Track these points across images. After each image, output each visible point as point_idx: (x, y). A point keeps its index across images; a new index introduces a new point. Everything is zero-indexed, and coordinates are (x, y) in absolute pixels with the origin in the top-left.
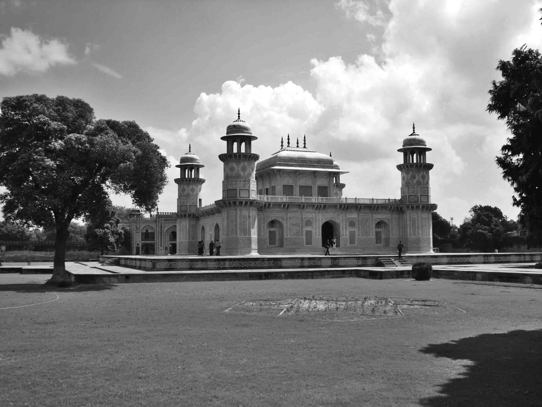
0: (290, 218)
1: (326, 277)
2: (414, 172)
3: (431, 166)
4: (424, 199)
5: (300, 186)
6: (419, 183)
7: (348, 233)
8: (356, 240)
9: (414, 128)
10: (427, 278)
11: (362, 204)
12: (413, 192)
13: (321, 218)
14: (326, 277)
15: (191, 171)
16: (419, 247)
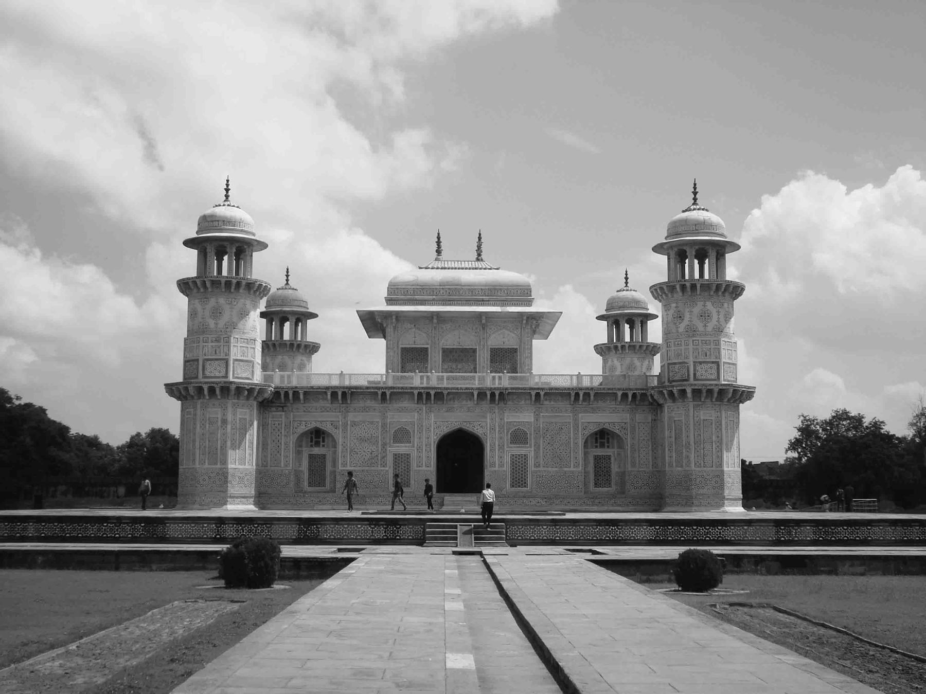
0: (354, 424)
1: (154, 567)
2: (680, 304)
3: (736, 290)
4: (702, 371)
5: (445, 351)
6: (692, 331)
7: (507, 459)
9: (695, 193)
10: (267, 583)
11: (542, 389)
12: (679, 355)
13: (436, 424)
14: (154, 567)
15: (296, 325)
16: (691, 497)
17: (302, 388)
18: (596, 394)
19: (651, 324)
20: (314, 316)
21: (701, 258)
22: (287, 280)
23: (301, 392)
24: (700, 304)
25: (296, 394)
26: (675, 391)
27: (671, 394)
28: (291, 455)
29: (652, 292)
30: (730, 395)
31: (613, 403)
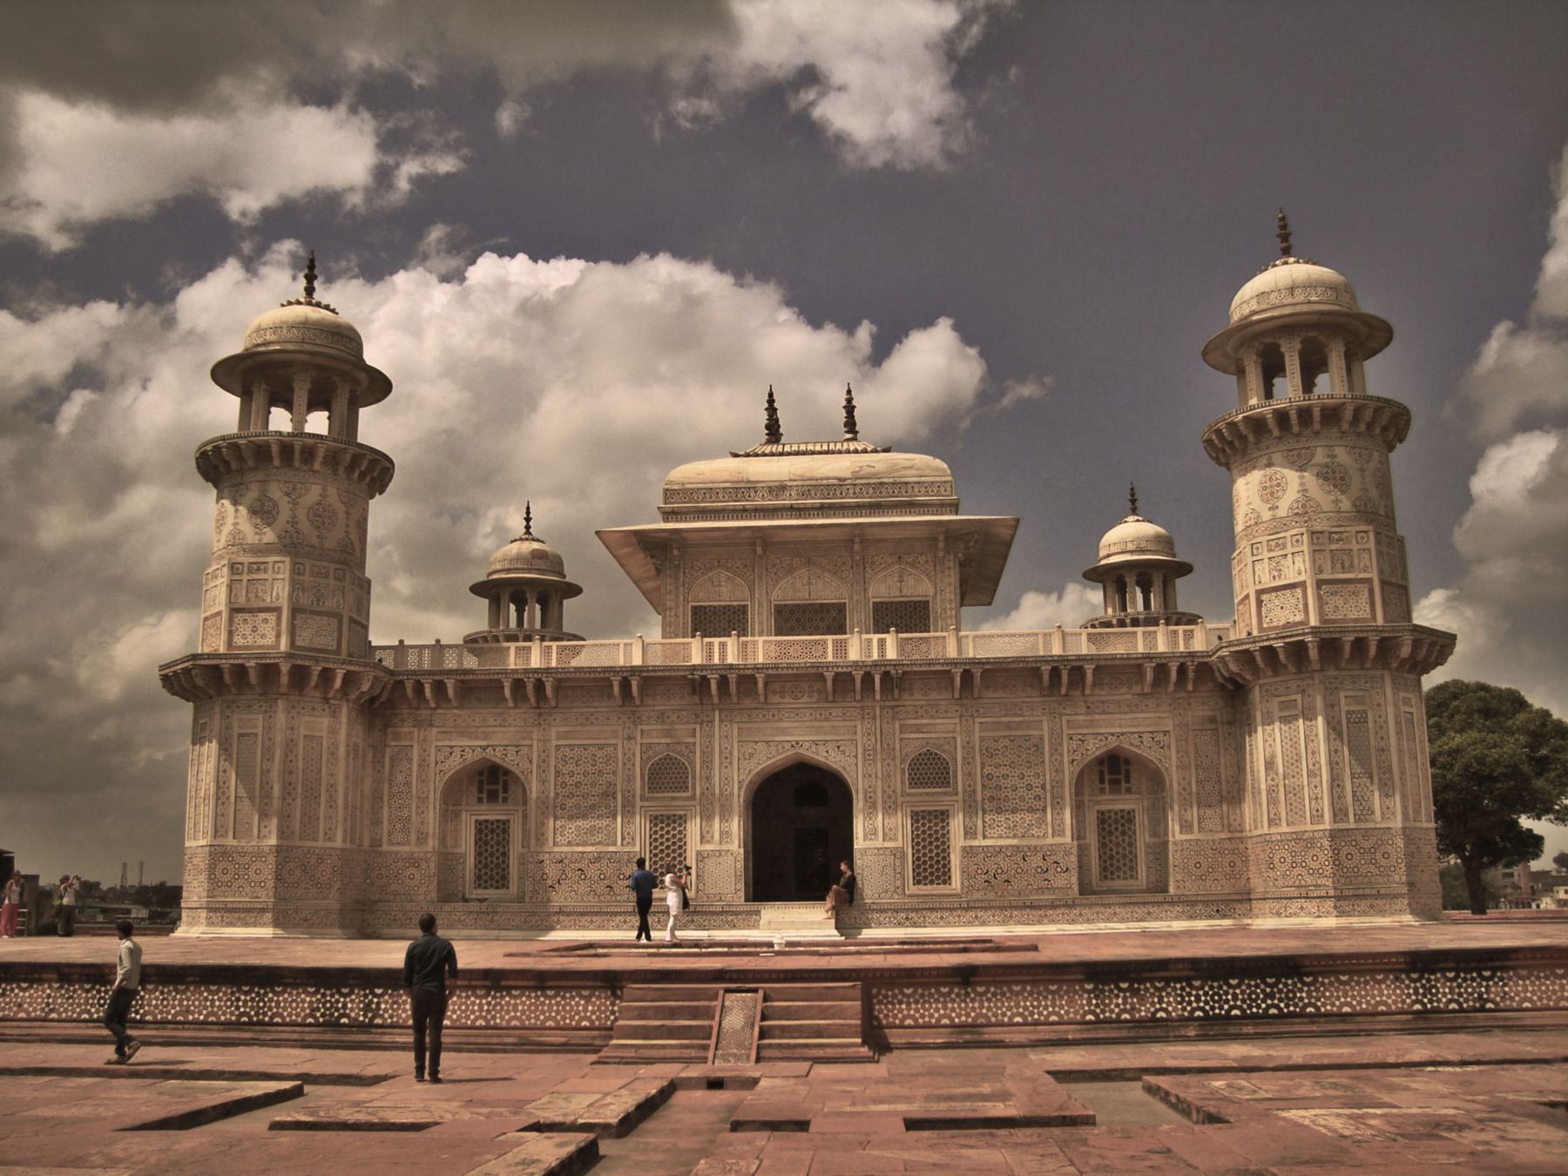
8: (955, 860)
9: (1285, 237)
17: (450, 672)
18: (1098, 670)
19: (1180, 583)
20: (574, 591)
21: (1311, 369)
22: (528, 527)
23: (450, 684)
24: (1320, 456)
25: (439, 687)
26: (1278, 644)
27: (1269, 652)
28: (432, 818)
29: (1209, 442)
30: (1405, 651)
31: (1137, 689)
